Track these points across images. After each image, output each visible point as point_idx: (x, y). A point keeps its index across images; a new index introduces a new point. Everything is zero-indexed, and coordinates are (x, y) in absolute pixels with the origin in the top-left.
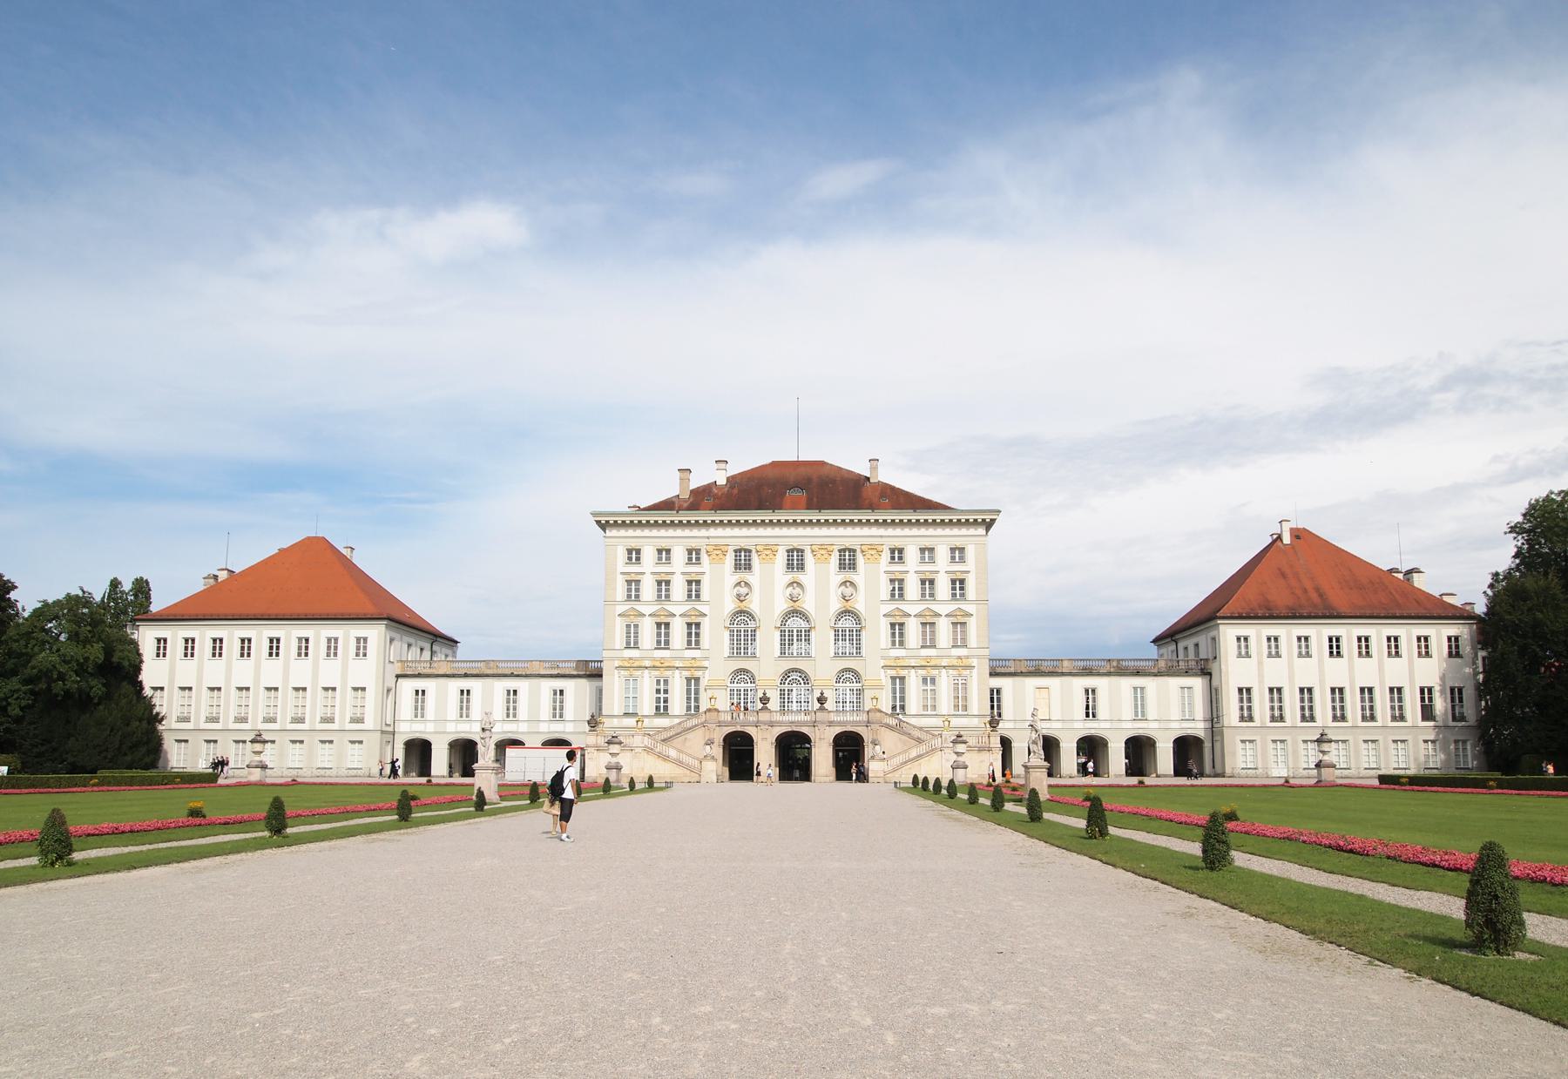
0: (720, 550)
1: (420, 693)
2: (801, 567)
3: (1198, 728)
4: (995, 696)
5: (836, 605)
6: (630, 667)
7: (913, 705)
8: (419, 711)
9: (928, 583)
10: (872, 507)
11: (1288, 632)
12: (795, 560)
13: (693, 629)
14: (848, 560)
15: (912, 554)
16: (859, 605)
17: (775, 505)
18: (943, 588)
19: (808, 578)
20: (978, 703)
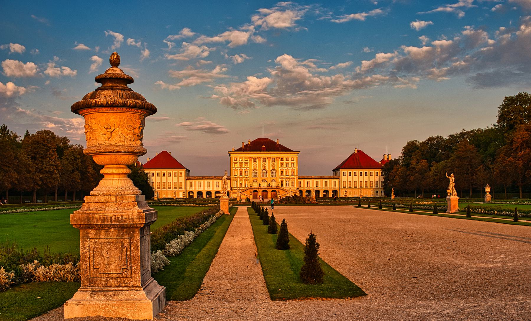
0: (250, 159)
1: (191, 183)
2: (265, 161)
3: (337, 188)
4: (300, 182)
5: (271, 168)
6: (236, 179)
7: (285, 185)
8: (191, 186)
9: (287, 165)
10: (278, 151)
11: (352, 171)
12: (264, 161)
13: (246, 172)
14: (273, 161)
15: (285, 159)
16: (276, 168)
17: (261, 151)
18: (290, 165)
19: (267, 163)
20: (296, 185)
